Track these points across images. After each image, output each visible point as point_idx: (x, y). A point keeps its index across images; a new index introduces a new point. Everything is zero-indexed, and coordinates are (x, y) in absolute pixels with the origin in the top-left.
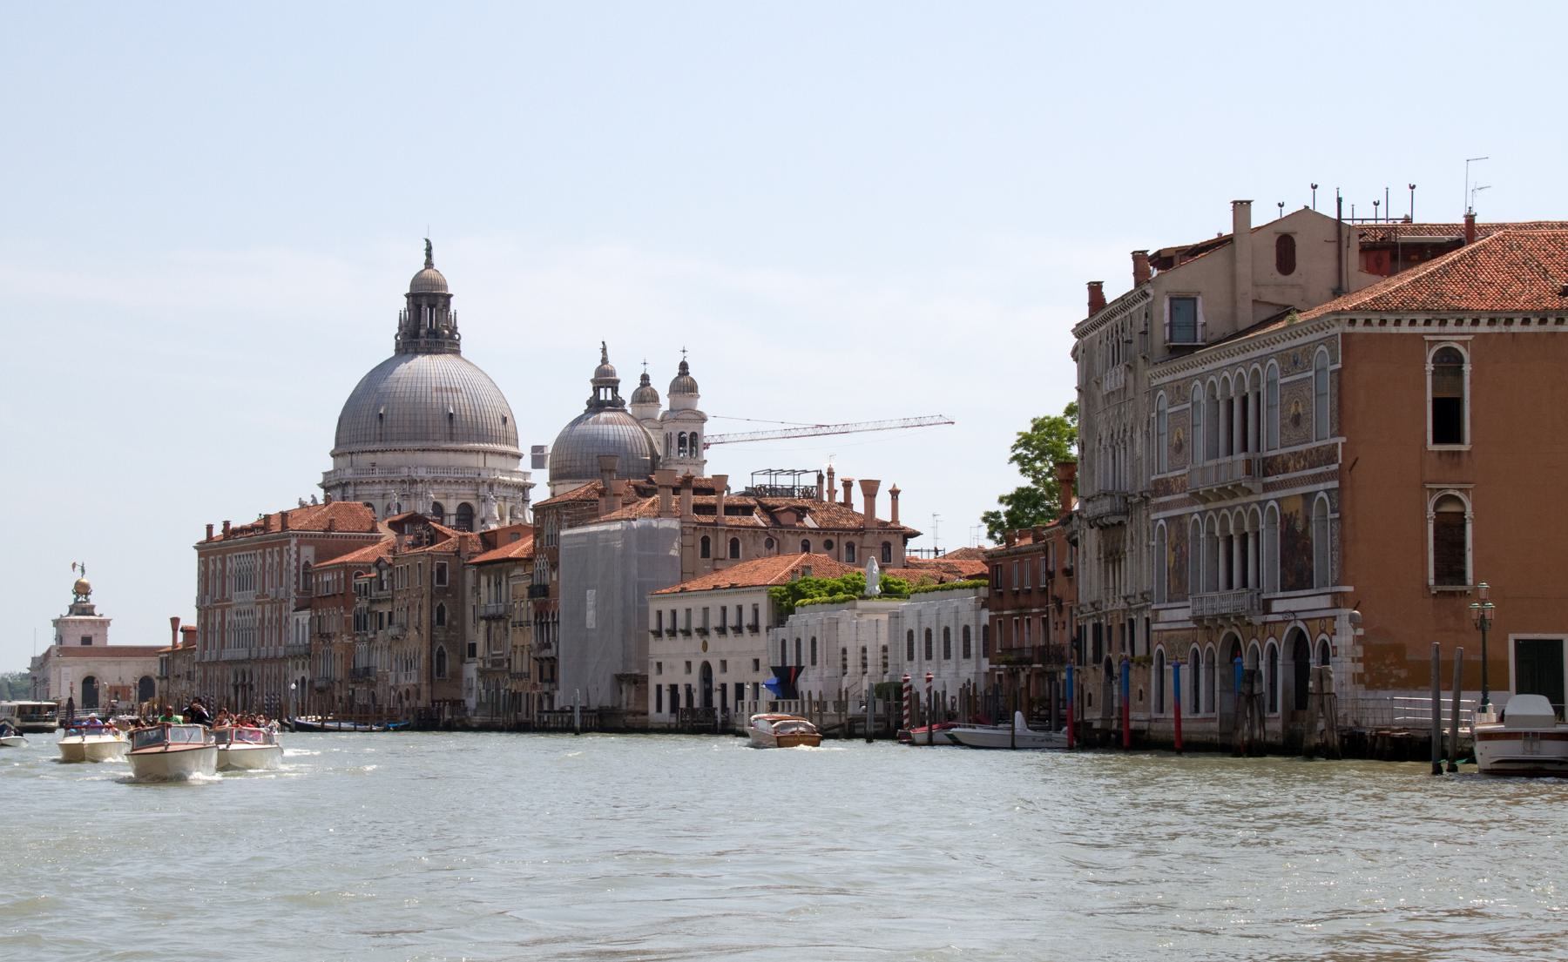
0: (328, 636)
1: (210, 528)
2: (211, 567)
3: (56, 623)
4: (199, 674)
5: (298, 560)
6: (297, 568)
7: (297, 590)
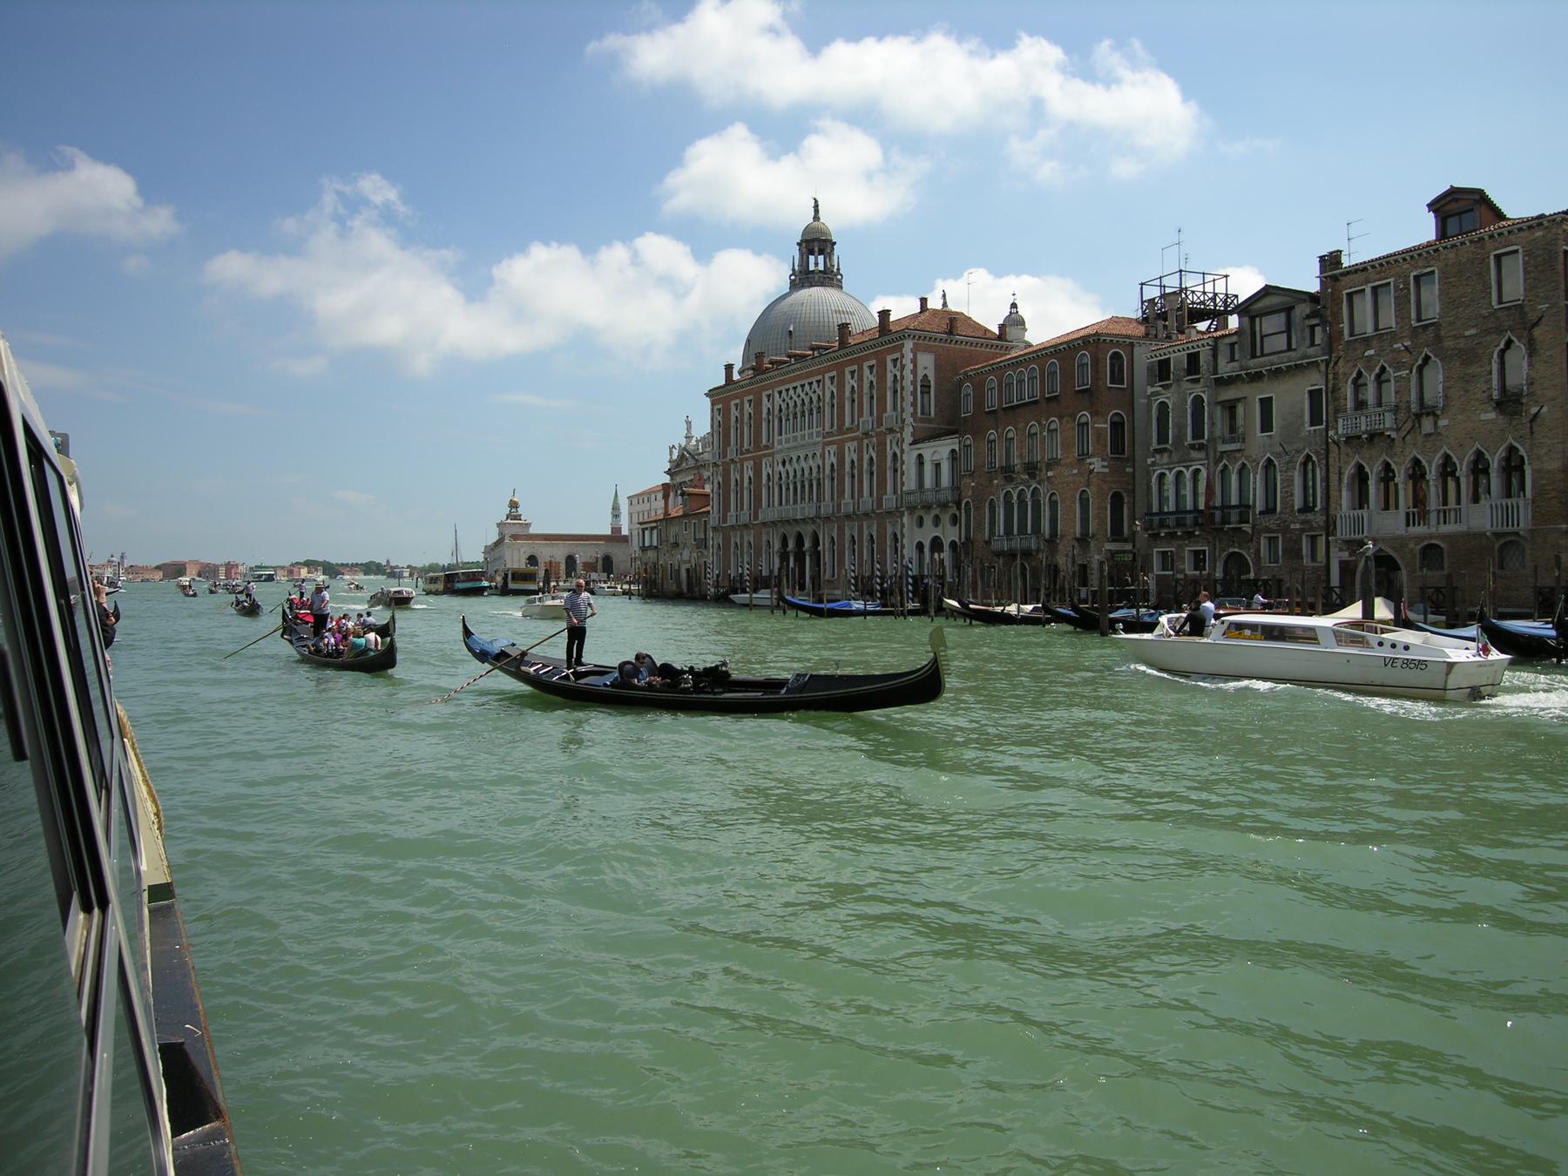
0: (1031, 469)
1: (729, 368)
2: (734, 413)
3: (499, 525)
4: (715, 540)
5: (914, 372)
6: (914, 383)
7: (914, 415)
